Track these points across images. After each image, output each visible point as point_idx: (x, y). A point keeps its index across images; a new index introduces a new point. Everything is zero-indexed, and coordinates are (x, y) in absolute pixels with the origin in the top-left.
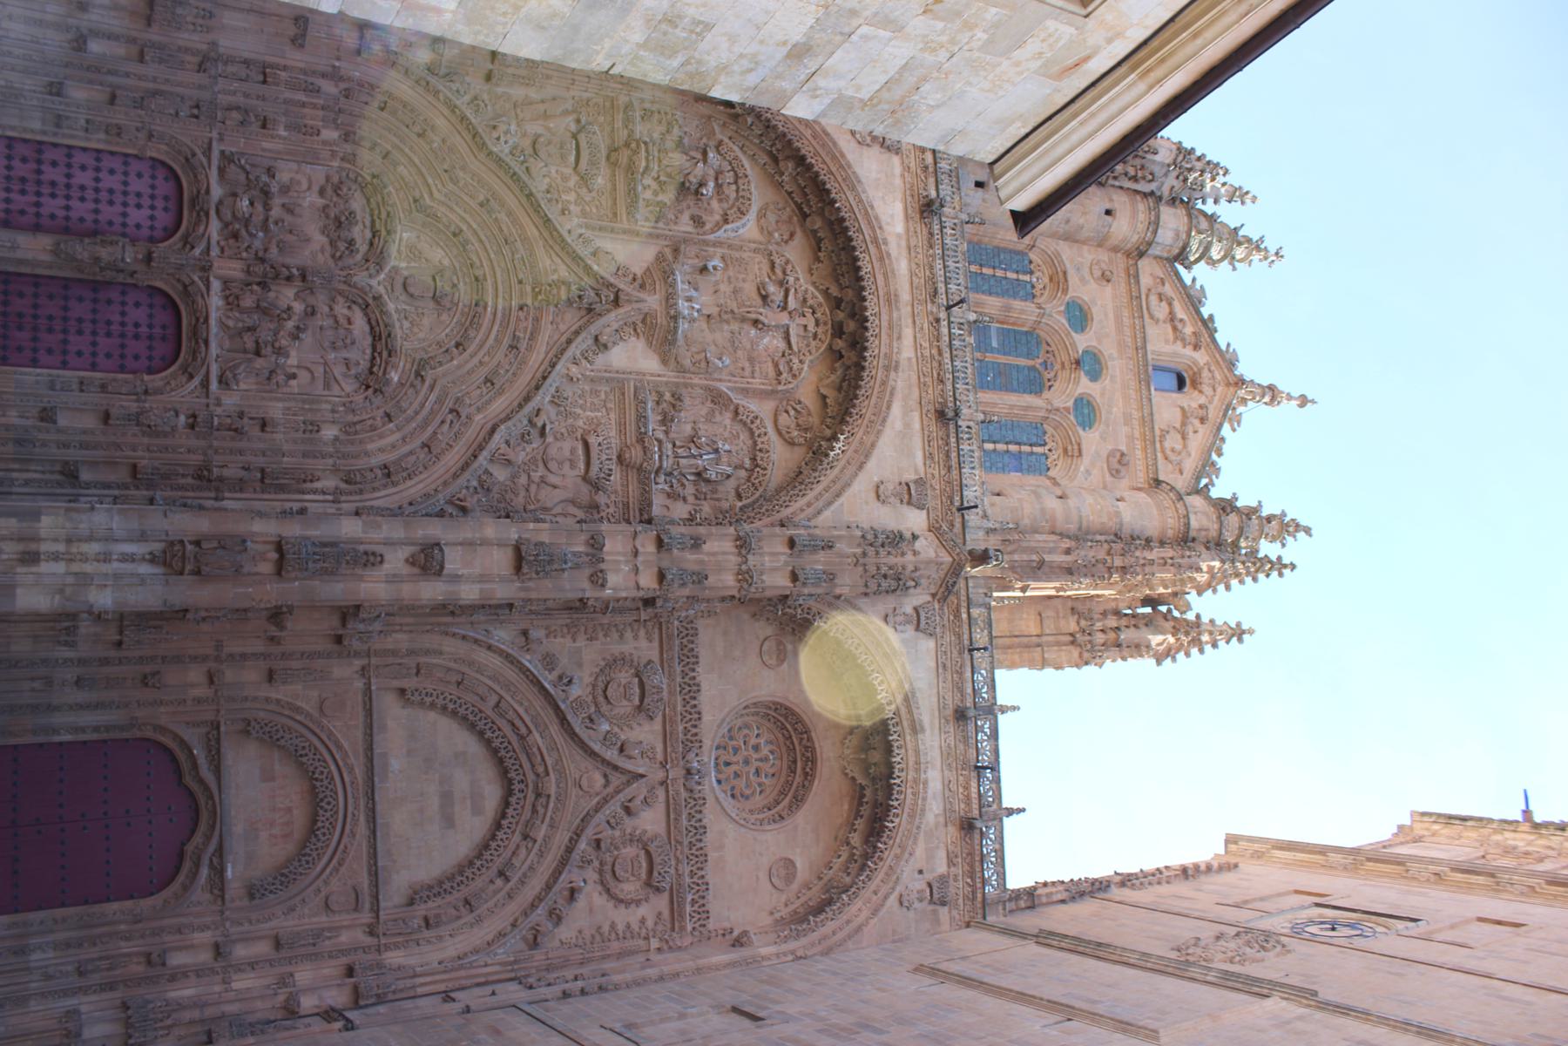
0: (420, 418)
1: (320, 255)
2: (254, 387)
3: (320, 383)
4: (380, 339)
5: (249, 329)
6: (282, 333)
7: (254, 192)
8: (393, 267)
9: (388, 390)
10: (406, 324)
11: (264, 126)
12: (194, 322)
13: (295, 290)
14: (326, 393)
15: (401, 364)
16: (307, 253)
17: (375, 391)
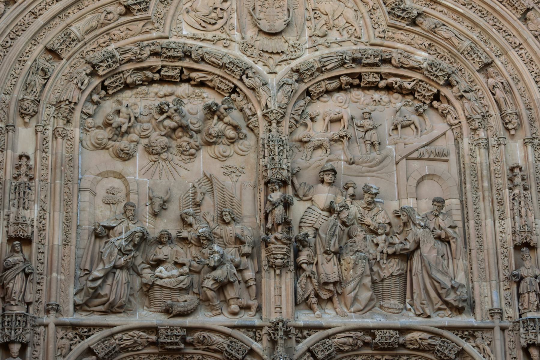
0: (481, 22)
1: (229, 163)
2: (461, 263)
3: (439, 167)
4: (359, 76)
5: (371, 270)
6: (368, 220)
7: (139, 260)
8: (244, 51)
9: (445, 64)
10: (334, 36)
11: (27, 241)
12: (370, 352)
13: (295, 200)
14: (453, 157)
15: (399, 45)
16: (228, 182)
17: (449, 84)
